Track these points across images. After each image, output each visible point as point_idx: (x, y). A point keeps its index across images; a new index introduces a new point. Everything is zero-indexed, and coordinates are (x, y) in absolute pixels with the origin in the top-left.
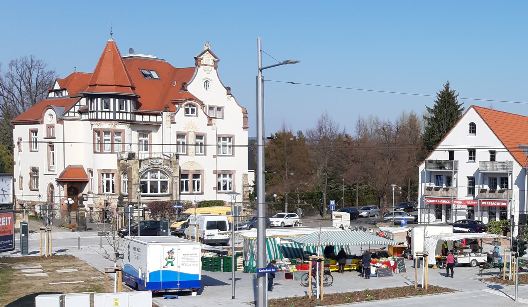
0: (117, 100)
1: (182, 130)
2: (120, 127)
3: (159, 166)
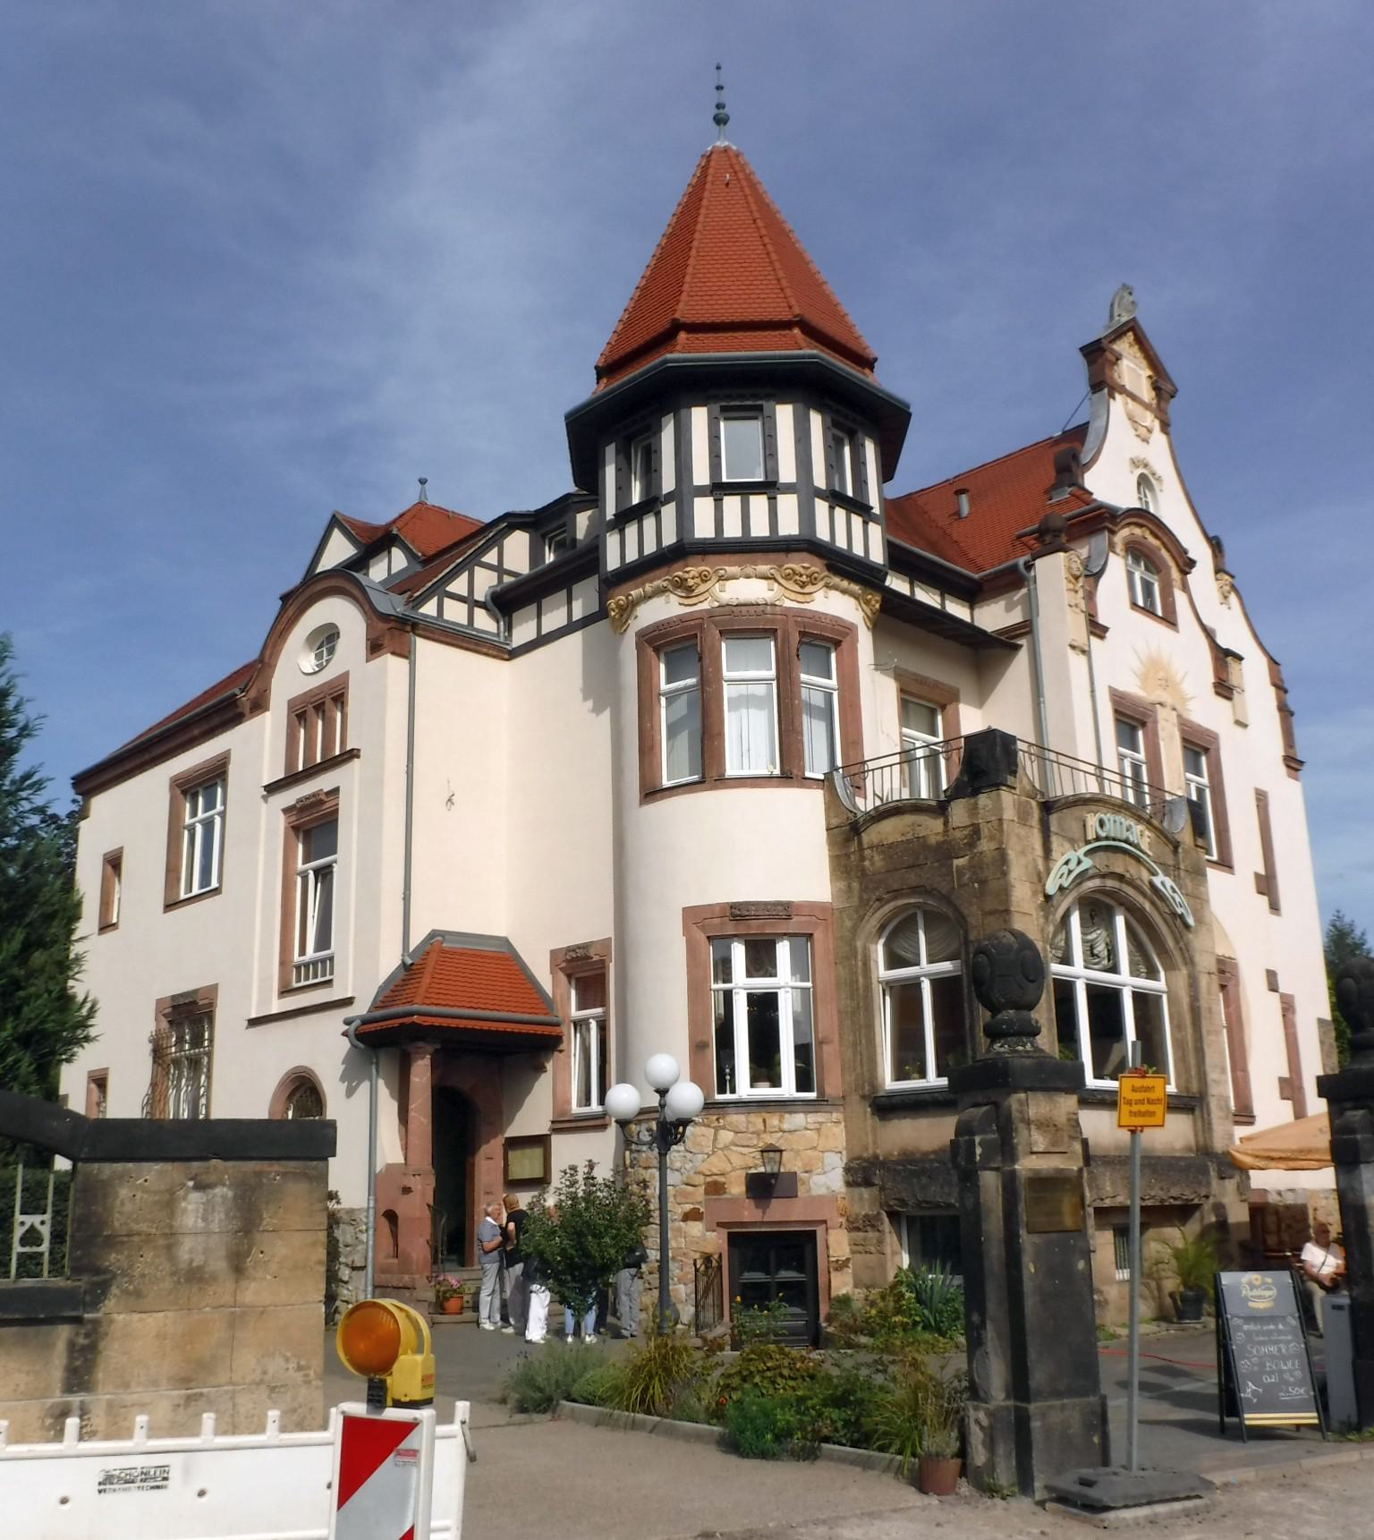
0: (816, 420)
2: (837, 604)
3: (1133, 870)
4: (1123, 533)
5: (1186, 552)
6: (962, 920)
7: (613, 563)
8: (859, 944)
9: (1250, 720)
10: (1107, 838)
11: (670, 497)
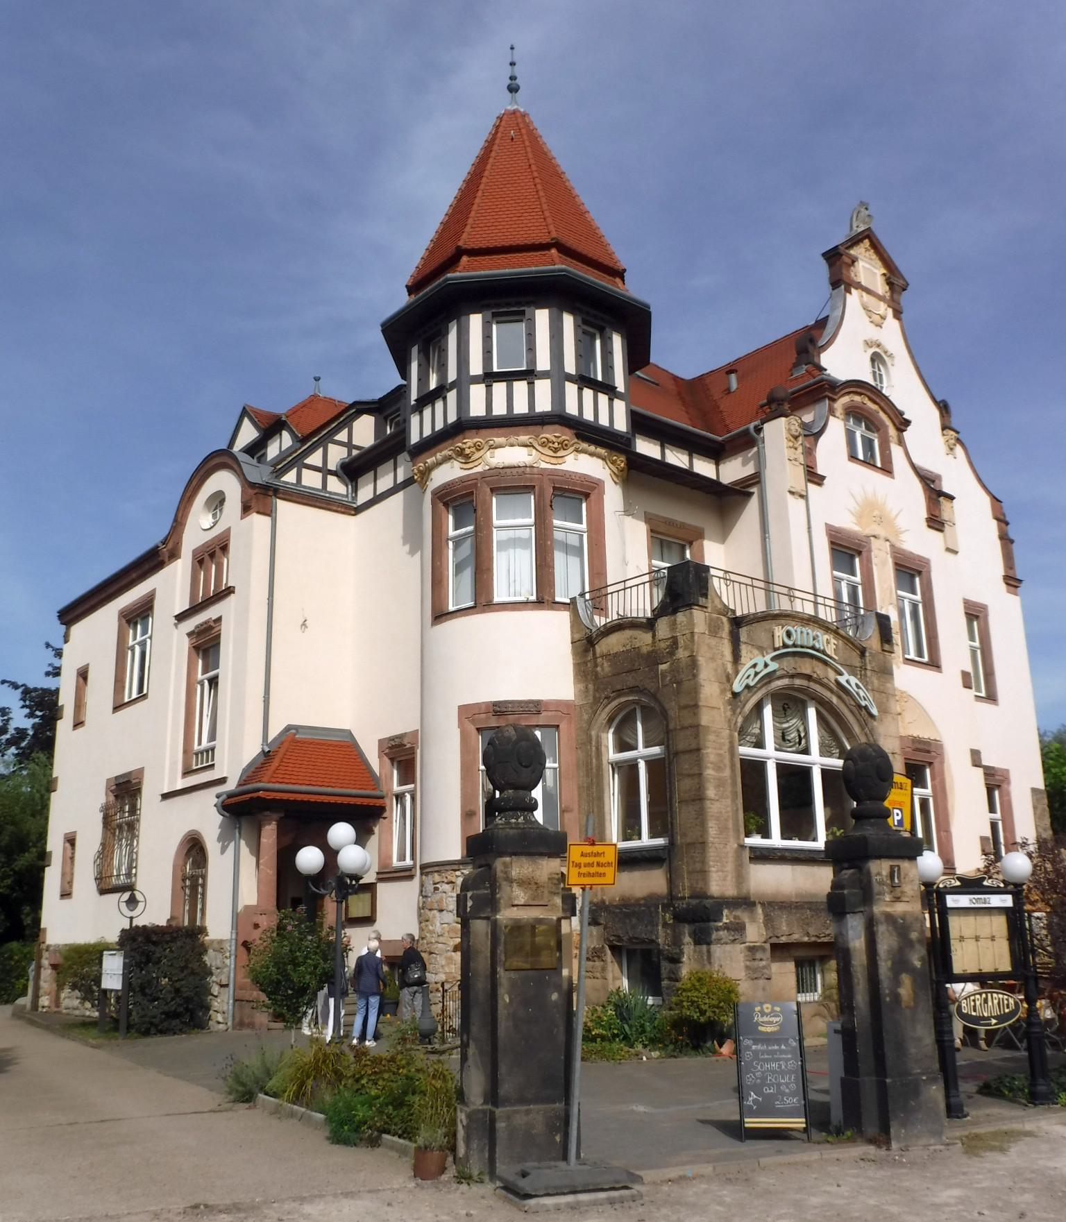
0: (568, 321)
1: (847, 522)
3: (819, 670)
4: (845, 400)
5: (902, 414)
6: (664, 714)
7: (414, 438)
8: (593, 733)
9: (961, 548)
10: (795, 646)
11: (453, 385)
